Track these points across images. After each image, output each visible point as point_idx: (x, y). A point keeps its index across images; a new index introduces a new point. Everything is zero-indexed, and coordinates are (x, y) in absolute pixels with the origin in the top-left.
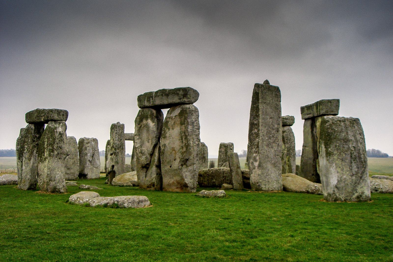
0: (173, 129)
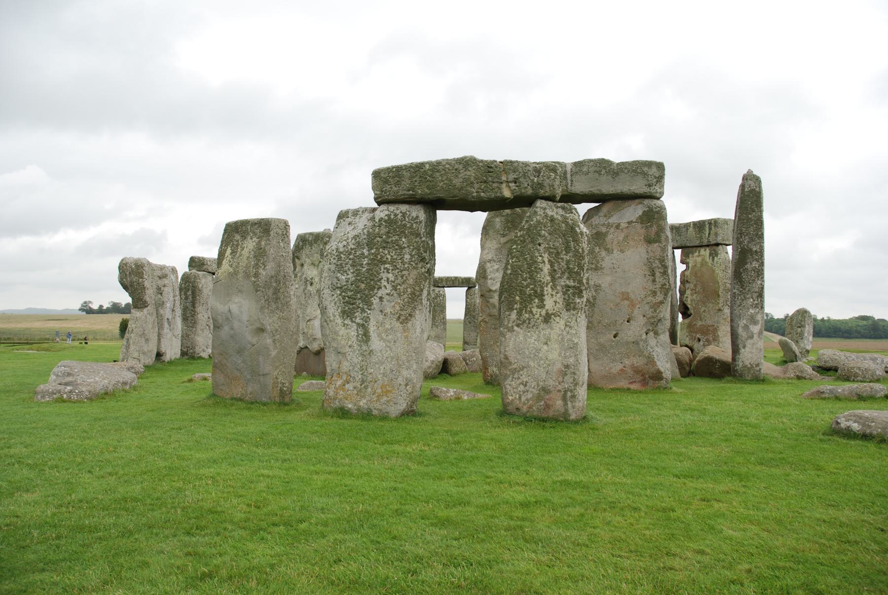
0: (622, 251)
